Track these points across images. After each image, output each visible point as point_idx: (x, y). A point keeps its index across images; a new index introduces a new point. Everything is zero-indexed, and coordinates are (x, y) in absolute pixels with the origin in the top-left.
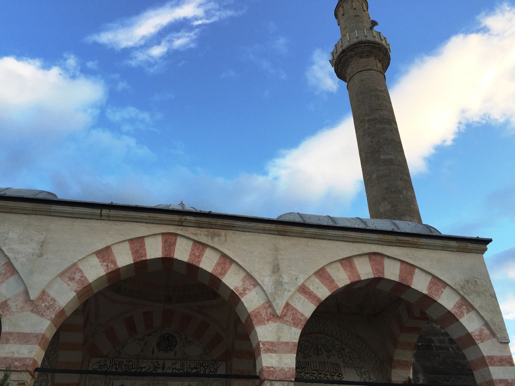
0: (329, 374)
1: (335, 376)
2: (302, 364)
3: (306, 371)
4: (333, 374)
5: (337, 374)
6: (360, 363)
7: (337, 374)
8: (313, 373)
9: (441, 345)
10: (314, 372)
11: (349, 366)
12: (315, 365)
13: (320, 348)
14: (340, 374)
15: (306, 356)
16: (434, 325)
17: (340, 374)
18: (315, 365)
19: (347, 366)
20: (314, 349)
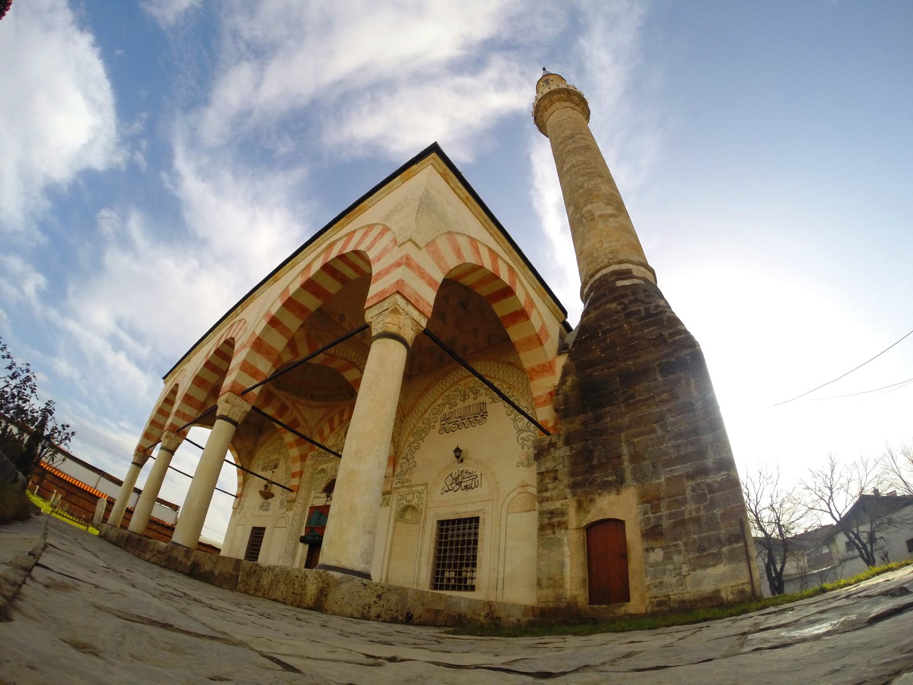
0: (473, 416)
1: (478, 417)
2: (447, 416)
3: (450, 422)
4: (478, 415)
5: (481, 414)
6: (509, 393)
7: (481, 414)
8: (457, 421)
9: (612, 326)
10: (458, 419)
11: (496, 401)
12: (459, 413)
13: (467, 393)
14: (484, 413)
15: (452, 405)
16: (608, 306)
17: (484, 413)
18: (459, 413)
19: (494, 402)
20: (461, 395)
